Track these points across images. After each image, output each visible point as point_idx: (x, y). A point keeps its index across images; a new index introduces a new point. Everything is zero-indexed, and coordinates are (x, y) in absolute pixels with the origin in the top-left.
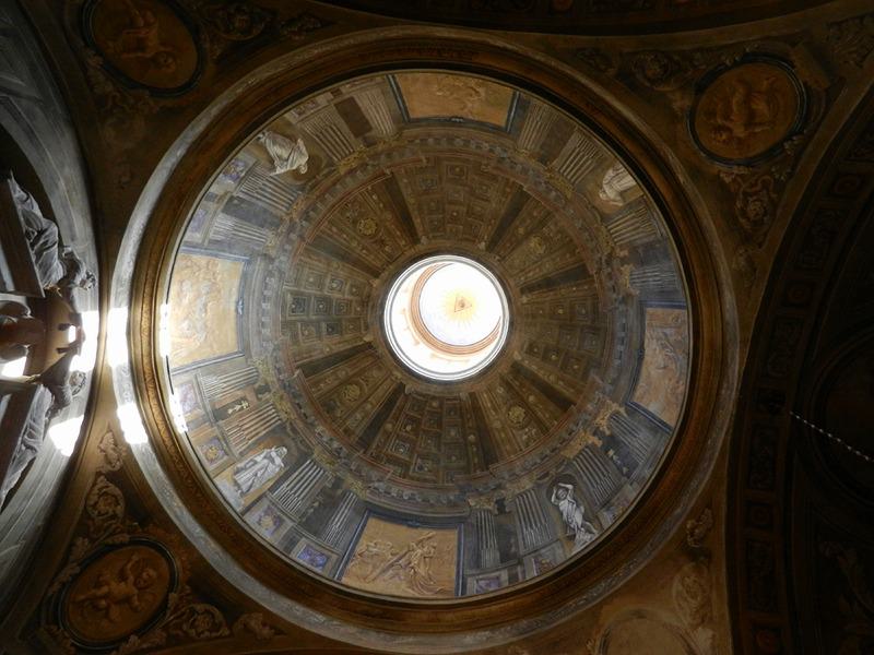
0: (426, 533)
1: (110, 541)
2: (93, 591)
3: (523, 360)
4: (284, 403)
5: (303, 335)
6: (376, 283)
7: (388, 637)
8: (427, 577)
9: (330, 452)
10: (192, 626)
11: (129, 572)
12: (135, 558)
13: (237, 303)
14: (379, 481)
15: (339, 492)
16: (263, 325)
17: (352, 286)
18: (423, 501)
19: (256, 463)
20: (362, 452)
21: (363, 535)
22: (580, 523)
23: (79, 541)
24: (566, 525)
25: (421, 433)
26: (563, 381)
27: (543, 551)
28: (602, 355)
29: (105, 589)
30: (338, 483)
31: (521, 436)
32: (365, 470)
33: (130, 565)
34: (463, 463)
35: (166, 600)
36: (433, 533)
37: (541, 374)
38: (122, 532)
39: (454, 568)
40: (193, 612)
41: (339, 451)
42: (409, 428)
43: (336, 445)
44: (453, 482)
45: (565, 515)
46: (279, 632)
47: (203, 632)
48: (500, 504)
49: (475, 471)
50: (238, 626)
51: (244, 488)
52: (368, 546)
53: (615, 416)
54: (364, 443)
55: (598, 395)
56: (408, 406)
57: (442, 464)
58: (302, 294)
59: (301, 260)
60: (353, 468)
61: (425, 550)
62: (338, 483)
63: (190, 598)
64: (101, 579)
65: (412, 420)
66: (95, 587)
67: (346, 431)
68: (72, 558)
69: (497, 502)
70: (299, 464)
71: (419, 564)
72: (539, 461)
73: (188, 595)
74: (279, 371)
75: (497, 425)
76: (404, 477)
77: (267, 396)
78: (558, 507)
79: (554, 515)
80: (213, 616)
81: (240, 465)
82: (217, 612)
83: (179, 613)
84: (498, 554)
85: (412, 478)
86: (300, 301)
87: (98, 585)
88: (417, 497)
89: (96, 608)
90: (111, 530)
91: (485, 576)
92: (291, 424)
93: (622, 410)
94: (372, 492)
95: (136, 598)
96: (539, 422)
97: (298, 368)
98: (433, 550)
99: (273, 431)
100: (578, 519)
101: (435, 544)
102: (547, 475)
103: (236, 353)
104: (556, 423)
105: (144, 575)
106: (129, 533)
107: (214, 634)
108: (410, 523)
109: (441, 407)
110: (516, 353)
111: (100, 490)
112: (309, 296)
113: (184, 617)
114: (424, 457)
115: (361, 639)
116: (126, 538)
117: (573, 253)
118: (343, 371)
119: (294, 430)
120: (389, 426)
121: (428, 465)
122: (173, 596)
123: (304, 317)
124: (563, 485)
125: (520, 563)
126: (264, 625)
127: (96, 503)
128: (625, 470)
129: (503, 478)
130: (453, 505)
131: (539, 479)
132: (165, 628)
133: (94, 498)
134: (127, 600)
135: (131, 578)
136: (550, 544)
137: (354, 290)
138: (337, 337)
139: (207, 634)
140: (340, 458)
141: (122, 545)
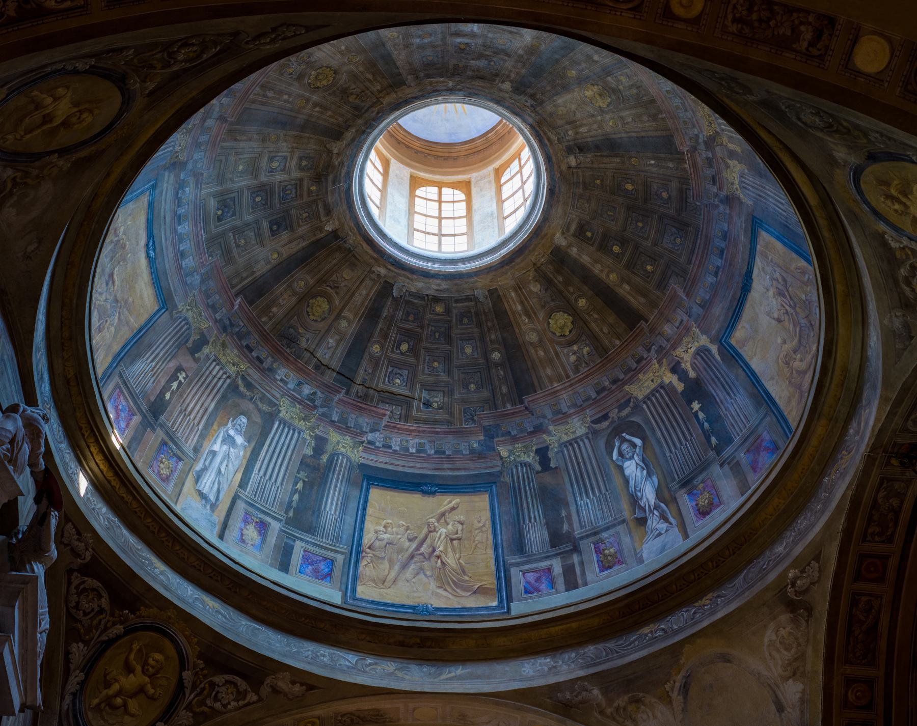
0: (447, 501)
1: (104, 638)
2: (105, 692)
3: (570, 246)
4: (228, 351)
5: (238, 246)
6: (336, 147)
7: (433, 670)
8: (460, 571)
9: (301, 402)
10: (216, 699)
11: (134, 663)
12: (135, 647)
13: (147, 246)
14: (372, 431)
15: (325, 458)
16: (183, 255)
17: (301, 159)
18: (436, 452)
19: (214, 453)
20: (344, 391)
21: (367, 518)
22: (652, 503)
23: (74, 648)
24: (634, 501)
25: (422, 352)
26: (628, 284)
27: (605, 535)
28: (689, 262)
29: (116, 687)
30: (320, 443)
31: (568, 356)
32: (353, 418)
33: (132, 657)
34: (486, 394)
35: (181, 680)
36: (456, 500)
37: (597, 269)
38: (114, 624)
39: (491, 553)
40: (213, 685)
41: (312, 397)
42: (404, 347)
43: (307, 390)
44: (474, 422)
45: (632, 483)
46: (311, 688)
47: (229, 703)
48: (543, 453)
49: (504, 405)
50: (265, 690)
51: (212, 498)
52: (376, 532)
53: (703, 352)
54: (346, 377)
55: (680, 315)
56: (400, 314)
57: (457, 396)
58: (230, 191)
59: (223, 148)
60: (335, 418)
61: (450, 527)
62: (320, 443)
63: (205, 672)
64: (108, 678)
65: (408, 335)
66: (105, 688)
67: (317, 367)
68: (72, 666)
69: (538, 452)
70: (264, 434)
71: (445, 552)
72: (593, 395)
73: (202, 670)
74: (213, 308)
75: (533, 337)
76: (406, 421)
77: (206, 350)
78: (621, 469)
79: (618, 481)
80: (235, 685)
81: (199, 466)
82: (238, 680)
83: (198, 690)
84: (546, 533)
85: (417, 421)
86: (227, 203)
87: (108, 685)
88: (427, 447)
89: (114, 707)
90: (102, 627)
91: (534, 566)
92: (243, 378)
93: (714, 349)
94: (366, 450)
95: (149, 686)
96: (595, 340)
97: (237, 295)
98: (460, 527)
99: (224, 397)
100: (649, 495)
101: (462, 518)
102: (605, 417)
103: (158, 311)
104: (618, 342)
105: (151, 661)
106: (121, 623)
107: (241, 703)
108: (425, 488)
109: (448, 311)
110: (558, 235)
111: (77, 587)
112: (240, 192)
113: (205, 692)
114: (430, 388)
115: (404, 679)
116: (119, 629)
117: (654, 117)
118: (302, 281)
119: (249, 386)
120: (376, 348)
121: (437, 399)
122: (187, 675)
123: (238, 223)
124: (628, 437)
125: (576, 549)
126: (294, 683)
127: (78, 603)
128: (714, 440)
129: (544, 417)
130: (477, 456)
131: (593, 422)
132: (189, 707)
133: (74, 598)
134: (141, 690)
135: (139, 668)
136: (614, 526)
137: (304, 163)
138: (285, 236)
139: (234, 704)
140: (315, 407)
141: (118, 637)
